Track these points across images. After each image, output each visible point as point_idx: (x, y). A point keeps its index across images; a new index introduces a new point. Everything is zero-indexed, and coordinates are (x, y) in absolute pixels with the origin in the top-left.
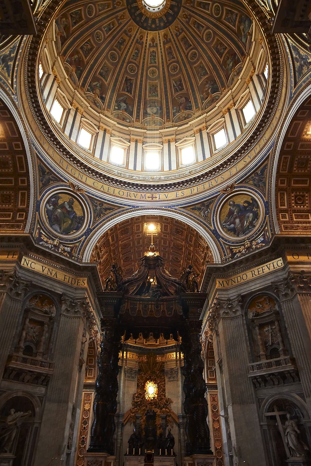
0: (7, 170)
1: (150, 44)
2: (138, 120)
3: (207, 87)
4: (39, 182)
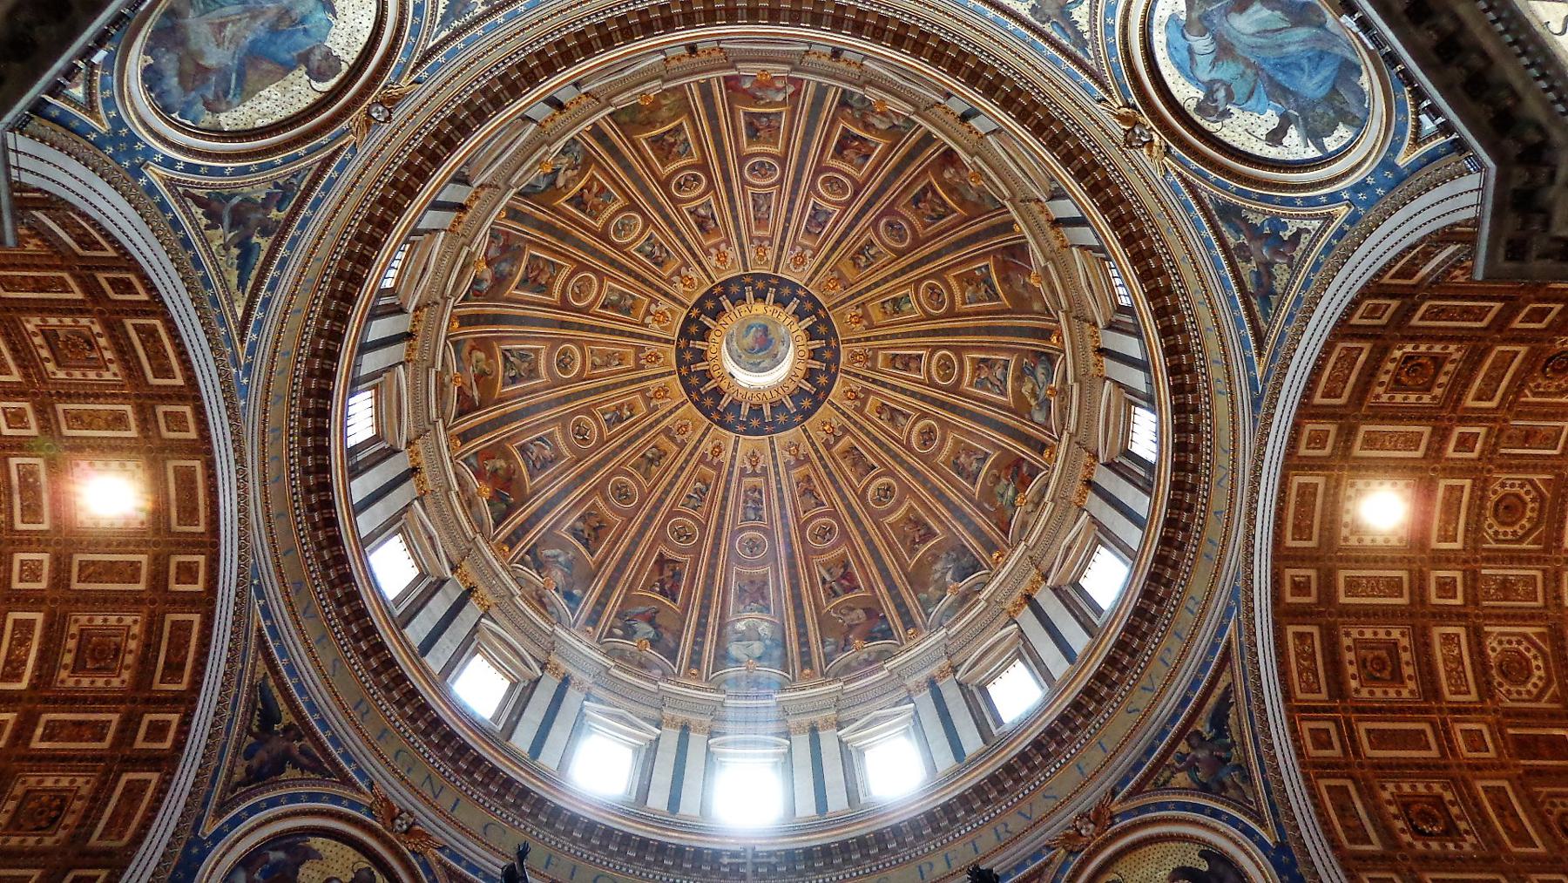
0: (100, 683)
1: (743, 470)
2: (695, 671)
3: (936, 571)
4: (235, 755)
